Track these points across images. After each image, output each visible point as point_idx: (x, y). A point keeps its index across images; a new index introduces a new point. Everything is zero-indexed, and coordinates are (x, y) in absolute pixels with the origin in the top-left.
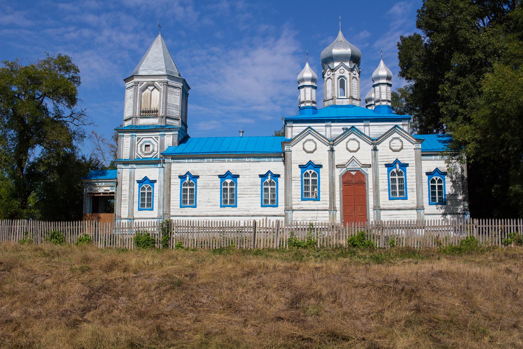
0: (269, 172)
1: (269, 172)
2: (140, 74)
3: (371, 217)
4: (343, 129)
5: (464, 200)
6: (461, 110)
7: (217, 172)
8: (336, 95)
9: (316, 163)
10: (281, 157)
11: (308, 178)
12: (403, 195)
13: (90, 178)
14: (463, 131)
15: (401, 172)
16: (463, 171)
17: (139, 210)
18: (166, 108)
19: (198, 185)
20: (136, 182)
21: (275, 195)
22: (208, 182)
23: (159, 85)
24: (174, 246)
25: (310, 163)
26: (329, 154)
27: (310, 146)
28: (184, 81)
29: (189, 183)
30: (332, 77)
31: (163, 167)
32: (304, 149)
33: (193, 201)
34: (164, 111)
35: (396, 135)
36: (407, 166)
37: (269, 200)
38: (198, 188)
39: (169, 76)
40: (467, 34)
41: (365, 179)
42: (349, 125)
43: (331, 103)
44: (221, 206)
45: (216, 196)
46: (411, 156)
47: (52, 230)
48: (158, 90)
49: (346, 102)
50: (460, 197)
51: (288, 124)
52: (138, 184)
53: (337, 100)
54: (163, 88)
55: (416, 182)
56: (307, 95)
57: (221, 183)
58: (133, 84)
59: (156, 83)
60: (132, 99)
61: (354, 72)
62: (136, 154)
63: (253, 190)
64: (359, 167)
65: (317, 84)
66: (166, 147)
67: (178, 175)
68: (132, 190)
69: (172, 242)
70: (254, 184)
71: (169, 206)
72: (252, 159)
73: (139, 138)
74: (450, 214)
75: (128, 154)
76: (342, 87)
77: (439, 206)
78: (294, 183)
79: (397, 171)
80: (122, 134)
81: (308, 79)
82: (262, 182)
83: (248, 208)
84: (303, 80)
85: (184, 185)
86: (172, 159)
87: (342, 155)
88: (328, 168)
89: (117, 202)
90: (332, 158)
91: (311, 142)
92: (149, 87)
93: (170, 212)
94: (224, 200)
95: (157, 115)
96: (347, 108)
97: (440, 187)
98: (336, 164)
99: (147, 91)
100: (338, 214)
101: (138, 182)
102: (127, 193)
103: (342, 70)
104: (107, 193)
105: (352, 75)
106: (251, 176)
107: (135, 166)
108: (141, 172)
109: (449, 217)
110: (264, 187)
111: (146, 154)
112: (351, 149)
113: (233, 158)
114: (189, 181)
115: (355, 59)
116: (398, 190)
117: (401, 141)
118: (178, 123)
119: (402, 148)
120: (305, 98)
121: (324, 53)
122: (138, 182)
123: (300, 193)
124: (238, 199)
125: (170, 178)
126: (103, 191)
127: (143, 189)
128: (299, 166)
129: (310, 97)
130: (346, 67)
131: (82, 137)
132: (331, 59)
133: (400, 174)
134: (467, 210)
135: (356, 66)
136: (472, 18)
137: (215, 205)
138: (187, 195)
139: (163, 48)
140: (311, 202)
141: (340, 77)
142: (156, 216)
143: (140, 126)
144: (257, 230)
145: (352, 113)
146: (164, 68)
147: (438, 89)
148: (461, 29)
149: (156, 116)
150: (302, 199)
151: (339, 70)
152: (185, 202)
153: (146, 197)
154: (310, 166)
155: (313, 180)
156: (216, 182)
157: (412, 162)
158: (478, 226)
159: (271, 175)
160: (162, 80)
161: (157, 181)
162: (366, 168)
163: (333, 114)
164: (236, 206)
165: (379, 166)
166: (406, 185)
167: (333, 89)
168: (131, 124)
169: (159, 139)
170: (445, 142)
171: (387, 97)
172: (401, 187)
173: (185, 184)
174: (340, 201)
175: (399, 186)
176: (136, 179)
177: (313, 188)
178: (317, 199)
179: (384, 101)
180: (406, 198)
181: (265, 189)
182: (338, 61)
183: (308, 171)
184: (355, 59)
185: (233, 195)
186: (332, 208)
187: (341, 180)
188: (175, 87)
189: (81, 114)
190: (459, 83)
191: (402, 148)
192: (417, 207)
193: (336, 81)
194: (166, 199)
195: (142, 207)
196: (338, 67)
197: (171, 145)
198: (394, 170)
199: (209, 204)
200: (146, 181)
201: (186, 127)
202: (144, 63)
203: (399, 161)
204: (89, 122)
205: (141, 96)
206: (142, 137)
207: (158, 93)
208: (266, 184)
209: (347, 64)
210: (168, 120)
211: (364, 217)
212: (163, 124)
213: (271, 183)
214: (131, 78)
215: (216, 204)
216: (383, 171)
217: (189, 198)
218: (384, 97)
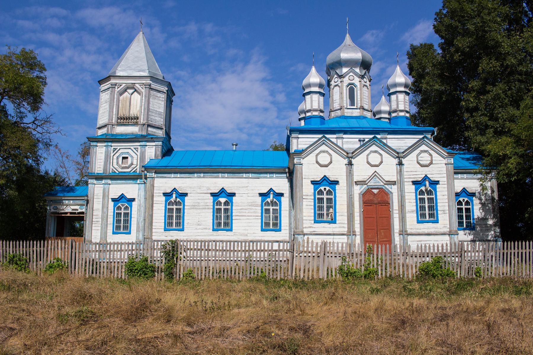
0: (271, 189)
1: (271, 189)
5: (495, 225)
7: (209, 189)
8: (345, 105)
9: (332, 179)
10: (286, 173)
12: (434, 218)
13: (55, 195)
14: (495, 146)
15: (430, 190)
16: (493, 191)
17: (114, 233)
18: (148, 115)
19: (186, 204)
20: (110, 200)
21: (277, 218)
22: (198, 201)
23: (141, 88)
24: (182, 276)
26: (347, 168)
27: (324, 159)
28: (169, 85)
29: (175, 201)
30: (340, 85)
31: (145, 183)
33: (180, 223)
34: (145, 118)
35: (424, 147)
36: (437, 184)
37: (271, 222)
38: (186, 207)
39: (153, 78)
40: (499, 37)
41: (389, 198)
43: (339, 113)
45: (208, 217)
46: (442, 172)
47: (10, 251)
48: (139, 94)
49: (356, 113)
50: (491, 222)
51: (293, 135)
52: (113, 203)
54: (145, 91)
55: (449, 202)
56: (314, 102)
57: (214, 202)
58: (109, 86)
59: (137, 85)
60: (108, 104)
61: (365, 79)
62: (111, 167)
63: (252, 211)
64: (382, 184)
65: (325, 90)
66: (147, 160)
67: (163, 192)
68: (105, 210)
69: (178, 271)
70: (252, 204)
71: (151, 229)
72: (250, 175)
73: (115, 149)
74: (479, 241)
75: (102, 167)
77: (468, 231)
79: (426, 190)
80: (95, 144)
81: (315, 85)
82: (262, 201)
83: (246, 232)
84: (309, 85)
85: (169, 204)
86: (156, 173)
87: (362, 170)
88: (345, 185)
89: (87, 223)
91: (326, 154)
92: (128, 90)
93: (152, 235)
94: (222, 220)
95: (137, 122)
96: (358, 120)
97: (468, 210)
98: (355, 180)
99: (126, 94)
100: (358, 240)
101: (114, 200)
103: (351, 77)
104: (75, 213)
106: (249, 195)
107: (109, 181)
108: (117, 189)
110: (264, 207)
111: (123, 168)
112: (372, 163)
114: (176, 199)
115: (365, 65)
116: (428, 211)
117: (431, 155)
118: (161, 133)
119: (431, 163)
120: (312, 106)
121: (331, 58)
122: (114, 200)
123: (313, 215)
124: (234, 221)
125: (153, 196)
126: (70, 211)
127: (119, 208)
128: (312, 181)
129: (317, 105)
130: (356, 74)
131: (47, 145)
132: (340, 64)
133: (429, 193)
134: (498, 237)
135: (367, 73)
136: (501, 20)
137: (206, 229)
138: (172, 216)
139: (145, 46)
140: (326, 225)
141: (350, 84)
143: (117, 135)
144: (295, 254)
145: (364, 124)
146: (147, 68)
148: (491, 31)
149: (136, 124)
150: (316, 222)
151: (347, 77)
152: (170, 224)
153: (122, 218)
155: (327, 199)
157: (443, 180)
159: (274, 194)
160: (144, 82)
161: (136, 200)
162: (390, 186)
163: (343, 124)
164: (231, 230)
165: (406, 183)
166: (437, 206)
167: (341, 98)
168: (106, 132)
169: (139, 151)
170: (468, 159)
171: (405, 107)
172: (431, 208)
174: (360, 223)
175: (429, 207)
176: (110, 197)
177: (328, 208)
178: (333, 221)
181: (266, 209)
182: (347, 66)
184: (365, 65)
185: (228, 216)
186: (351, 233)
187: (361, 200)
189: (47, 121)
190: (488, 92)
191: (431, 163)
192: (450, 231)
193: (345, 88)
194: (147, 220)
195: (117, 230)
196: (347, 74)
197: (154, 158)
198: (423, 188)
199: (199, 227)
200: (123, 200)
201: (170, 138)
202: (122, 63)
203: (429, 178)
204: (55, 129)
205: (118, 100)
206: (119, 148)
208: (267, 204)
209: (357, 70)
210: (150, 129)
212: (144, 133)
213: (273, 203)
214: (108, 78)
215: (208, 227)
216: (410, 189)
217: (175, 218)
218: (401, 107)
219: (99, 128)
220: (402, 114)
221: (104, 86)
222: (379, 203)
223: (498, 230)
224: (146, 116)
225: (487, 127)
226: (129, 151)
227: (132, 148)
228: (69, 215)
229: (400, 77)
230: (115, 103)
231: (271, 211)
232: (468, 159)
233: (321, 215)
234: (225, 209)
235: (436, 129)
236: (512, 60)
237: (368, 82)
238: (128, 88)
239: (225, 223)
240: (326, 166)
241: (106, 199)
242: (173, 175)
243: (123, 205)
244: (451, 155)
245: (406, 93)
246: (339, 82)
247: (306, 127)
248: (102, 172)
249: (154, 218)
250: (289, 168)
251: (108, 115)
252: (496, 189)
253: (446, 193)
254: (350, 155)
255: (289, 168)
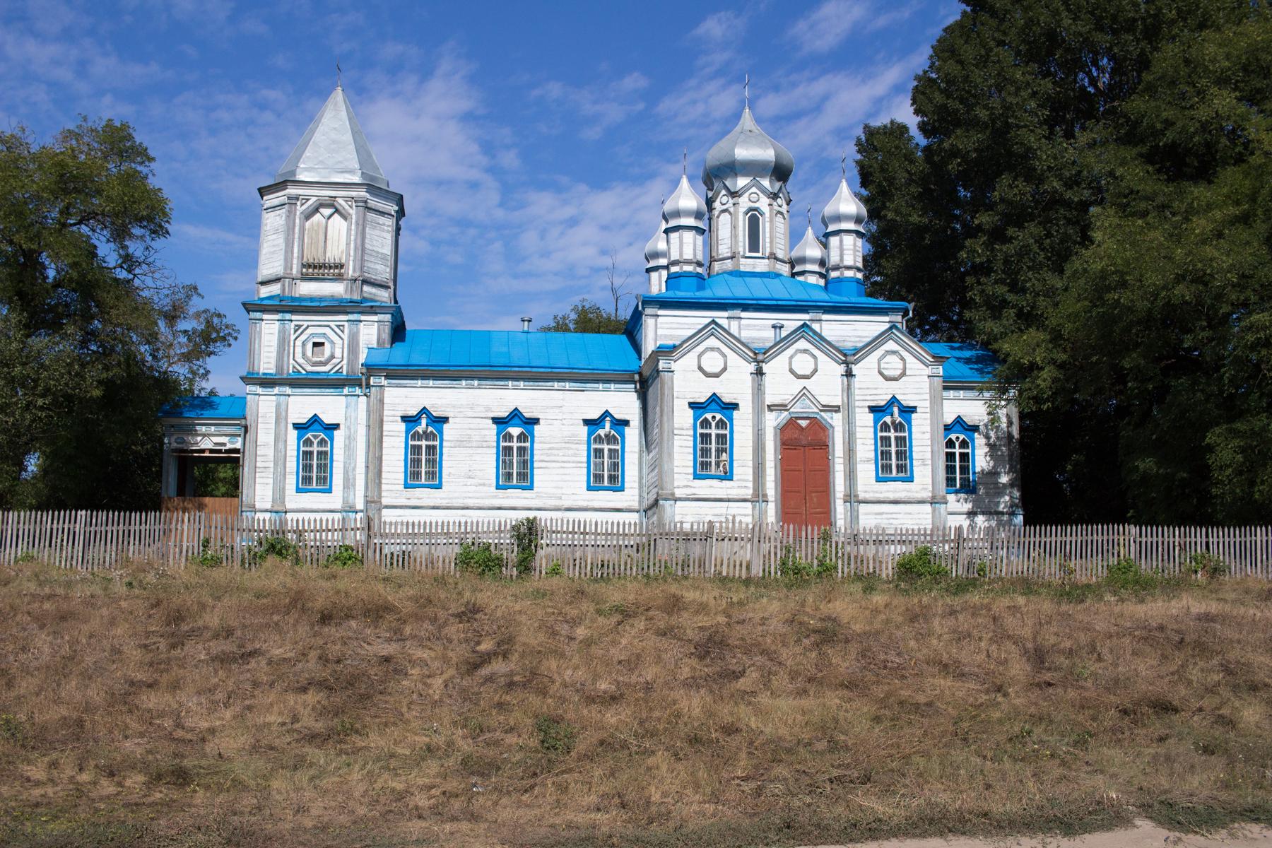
1: (607, 414)
2: (301, 177)
3: (838, 516)
4: (774, 327)
5: (1012, 484)
6: (1011, 297)
8: (741, 249)
10: (635, 383)
11: (708, 431)
12: (905, 472)
16: (1010, 423)
17: (299, 491)
19: (445, 437)
20: (290, 427)
22: (469, 432)
25: (714, 399)
27: (712, 362)
29: (425, 432)
30: (732, 210)
32: (700, 368)
34: (358, 267)
35: (891, 345)
37: (606, 475)
38: (445, 444)
39: (372, 188)
42: (792, 321)
43: (729, 265)
44: (498, 487)
45: (487, 463)
48: (345, 218)
49: (762, 266)
50: (1004, 479)
51: (648, 311)
52: (296, 432)
53: (743, 261)
56: (687, 246)
57: (498, 434)
62: (292, 361)
68: (281, 446)
70: (571, 440)
71: (380, 483)
72: (567, 385)
73: (299, 326)
74: (983, 513)
76: (756, 231)
77: (962, 495)
78: (678, 442)
79: (893, 422)
80: (258, 315)
81: (688, 213)
82: (590, 435)
83: (559, 491)
85: (413, 437)
86: (387, 377)
87: (780, 383)
88: (750, 410)
89: (246, 471)
90: (758, 390)
91: (716, 354)
92: (321, 210)
93: (380, 496)
97: (964, 457)
98: (768, 402)
99: (318, 216)
102: (270, 452)
103: (753, 195)
104: (220, 451)
105: (776, 207)
107: (288, 390)
108: (304, 405)
109: (980, 519)
110: (593, 446)
112: (799, 372)
113: (524, 379)
114: (426, 431)
115: (781, 172)
116: (894, 461)
117: (903, 359)
119: (903, 374)
120: (681, 254)
121: (715, 155)
123: (692, 464)
125: (382, 421)
126: (211, 446)
128: (690, 404)
129: (691, 252)
132: (732, 168)
133: (898, 427)
134: (1017, 506)
137: (484, 485)
140: (715, 482)
141: (751, 209)
142: (339, 506)
143: (301, 299)
145: (779, 291)
146: (357, 166)
147: (962, 247)
148: (1019, 127)
149: (339, 278)
150: (696, 477)
151: (747, 195)
152: (416, 475)
154: (713, 406)
156: (486, 432)
157: (923, 404)
158: (1138, 540)
160: (354, 194)
161: (342, 426)
163: (740, 290)
164: (531, 488)
166: (911, 452)
167: (734, 236)
172: (901, 455)
173: (416, 436)
175: (897, 453)
177: (720, 452)
178: (727, 476)
179: (849, 268)
180: (911, 480)
181: (596, 450)
183: (709, 416)
184: (781, 172)
185: (525, 462)
186: (758, 497)
188: (382, 213)
190: (1009, 240)
191: (903, 374)
192: (933, 497)
195: (305, 484)
196: (746, 188)
197: (375, 346)
198: (888, 419)
199: (470, 481)
200: (316, 426)
202: (307, 153)
203: (898, 401)
206: (306, 324)
207: (344, 224)
208: (599, 439)
209: (766, 183)
210: (366, 288)
211: (826, 515)
212: (356, 297)
213: (610, 439)
216: (865, 420)
217: (424, 464)
218: (849, 261)
219: (263, 283)
220: (849, 274)
221: (272, 200)
222: (809, 445)
223: (1017, 494)
224: (358, 264)
225: (1004, 303)
226: (327, 330)
227: (332, 324)
228: (207, 454)
229: (847, 202)
230: (297, 236)
231: (606, 452)
232: (968, 361)
233: (706, 465)
234: (519, 449)
235: (911, 306)
236: (1055, 184)
237: (785, 206)
238: (322, 205)
239: (519, 474)
240: (717, 376)
241: (283, 425)
242: (419, 382)
243: (315, 437)
244: (939, 359)
245: (857, 233)
246: (729, 205)
247: (671, 294)
248: (273, 371)
249: (384, 463)
250: (640, 374)
251: (282, 257)
252: (1015, 420)
253: (928, 429)
254: (760, 357)
255: (640, 374)
